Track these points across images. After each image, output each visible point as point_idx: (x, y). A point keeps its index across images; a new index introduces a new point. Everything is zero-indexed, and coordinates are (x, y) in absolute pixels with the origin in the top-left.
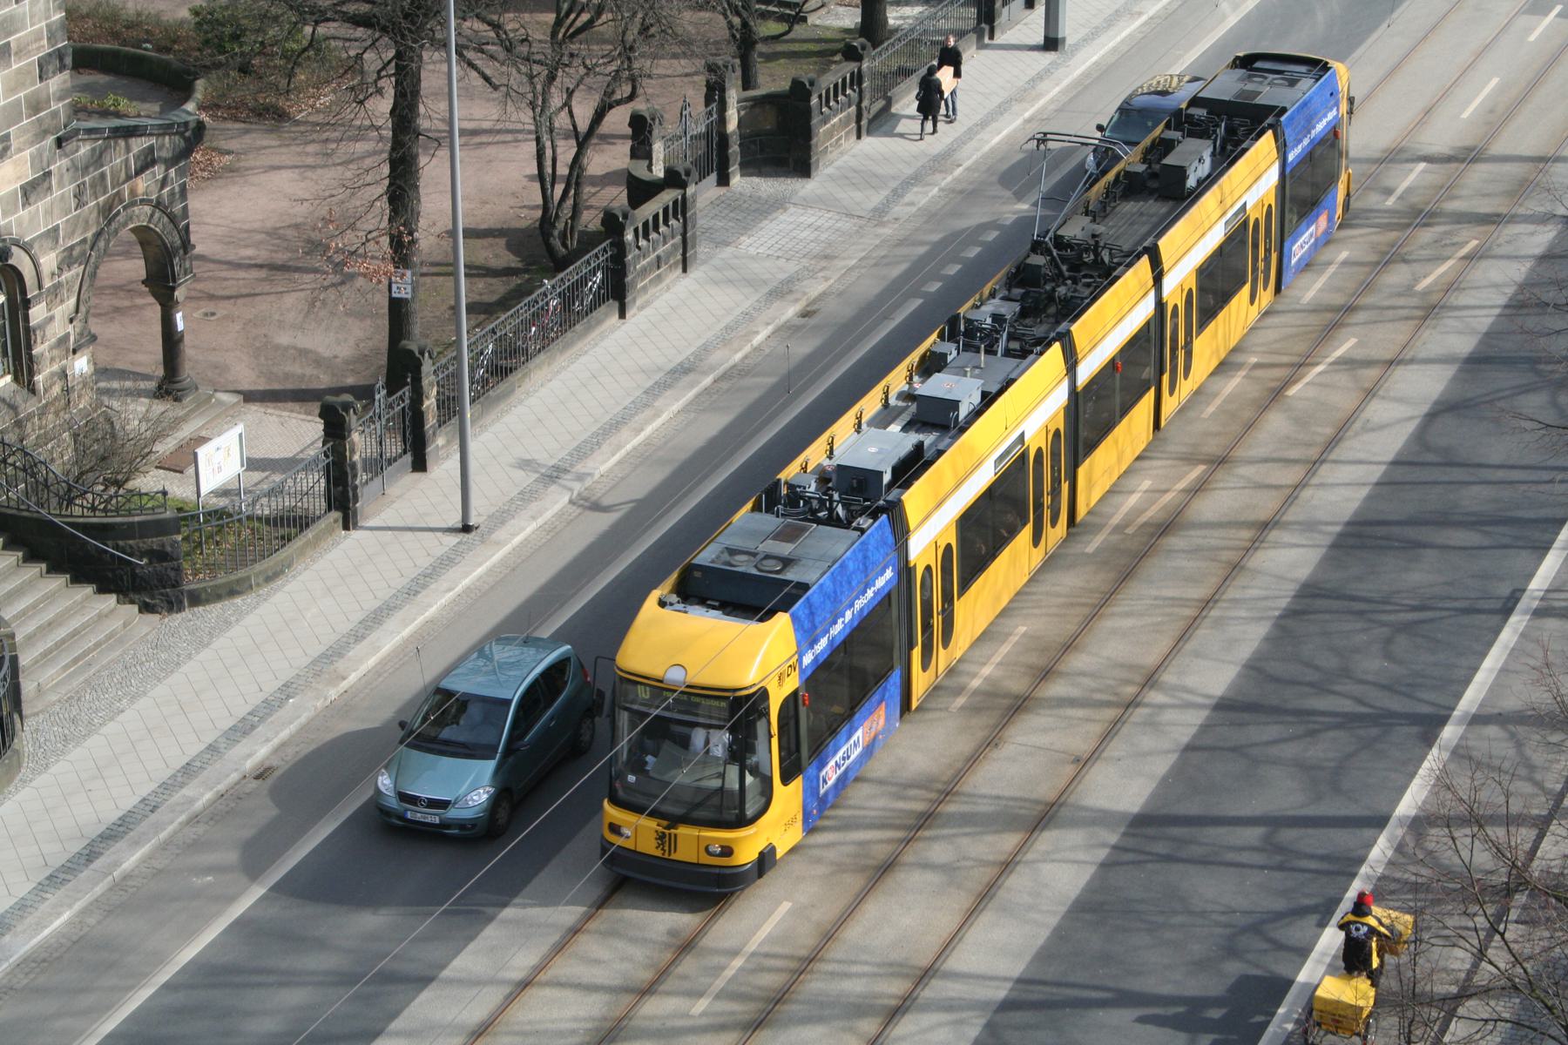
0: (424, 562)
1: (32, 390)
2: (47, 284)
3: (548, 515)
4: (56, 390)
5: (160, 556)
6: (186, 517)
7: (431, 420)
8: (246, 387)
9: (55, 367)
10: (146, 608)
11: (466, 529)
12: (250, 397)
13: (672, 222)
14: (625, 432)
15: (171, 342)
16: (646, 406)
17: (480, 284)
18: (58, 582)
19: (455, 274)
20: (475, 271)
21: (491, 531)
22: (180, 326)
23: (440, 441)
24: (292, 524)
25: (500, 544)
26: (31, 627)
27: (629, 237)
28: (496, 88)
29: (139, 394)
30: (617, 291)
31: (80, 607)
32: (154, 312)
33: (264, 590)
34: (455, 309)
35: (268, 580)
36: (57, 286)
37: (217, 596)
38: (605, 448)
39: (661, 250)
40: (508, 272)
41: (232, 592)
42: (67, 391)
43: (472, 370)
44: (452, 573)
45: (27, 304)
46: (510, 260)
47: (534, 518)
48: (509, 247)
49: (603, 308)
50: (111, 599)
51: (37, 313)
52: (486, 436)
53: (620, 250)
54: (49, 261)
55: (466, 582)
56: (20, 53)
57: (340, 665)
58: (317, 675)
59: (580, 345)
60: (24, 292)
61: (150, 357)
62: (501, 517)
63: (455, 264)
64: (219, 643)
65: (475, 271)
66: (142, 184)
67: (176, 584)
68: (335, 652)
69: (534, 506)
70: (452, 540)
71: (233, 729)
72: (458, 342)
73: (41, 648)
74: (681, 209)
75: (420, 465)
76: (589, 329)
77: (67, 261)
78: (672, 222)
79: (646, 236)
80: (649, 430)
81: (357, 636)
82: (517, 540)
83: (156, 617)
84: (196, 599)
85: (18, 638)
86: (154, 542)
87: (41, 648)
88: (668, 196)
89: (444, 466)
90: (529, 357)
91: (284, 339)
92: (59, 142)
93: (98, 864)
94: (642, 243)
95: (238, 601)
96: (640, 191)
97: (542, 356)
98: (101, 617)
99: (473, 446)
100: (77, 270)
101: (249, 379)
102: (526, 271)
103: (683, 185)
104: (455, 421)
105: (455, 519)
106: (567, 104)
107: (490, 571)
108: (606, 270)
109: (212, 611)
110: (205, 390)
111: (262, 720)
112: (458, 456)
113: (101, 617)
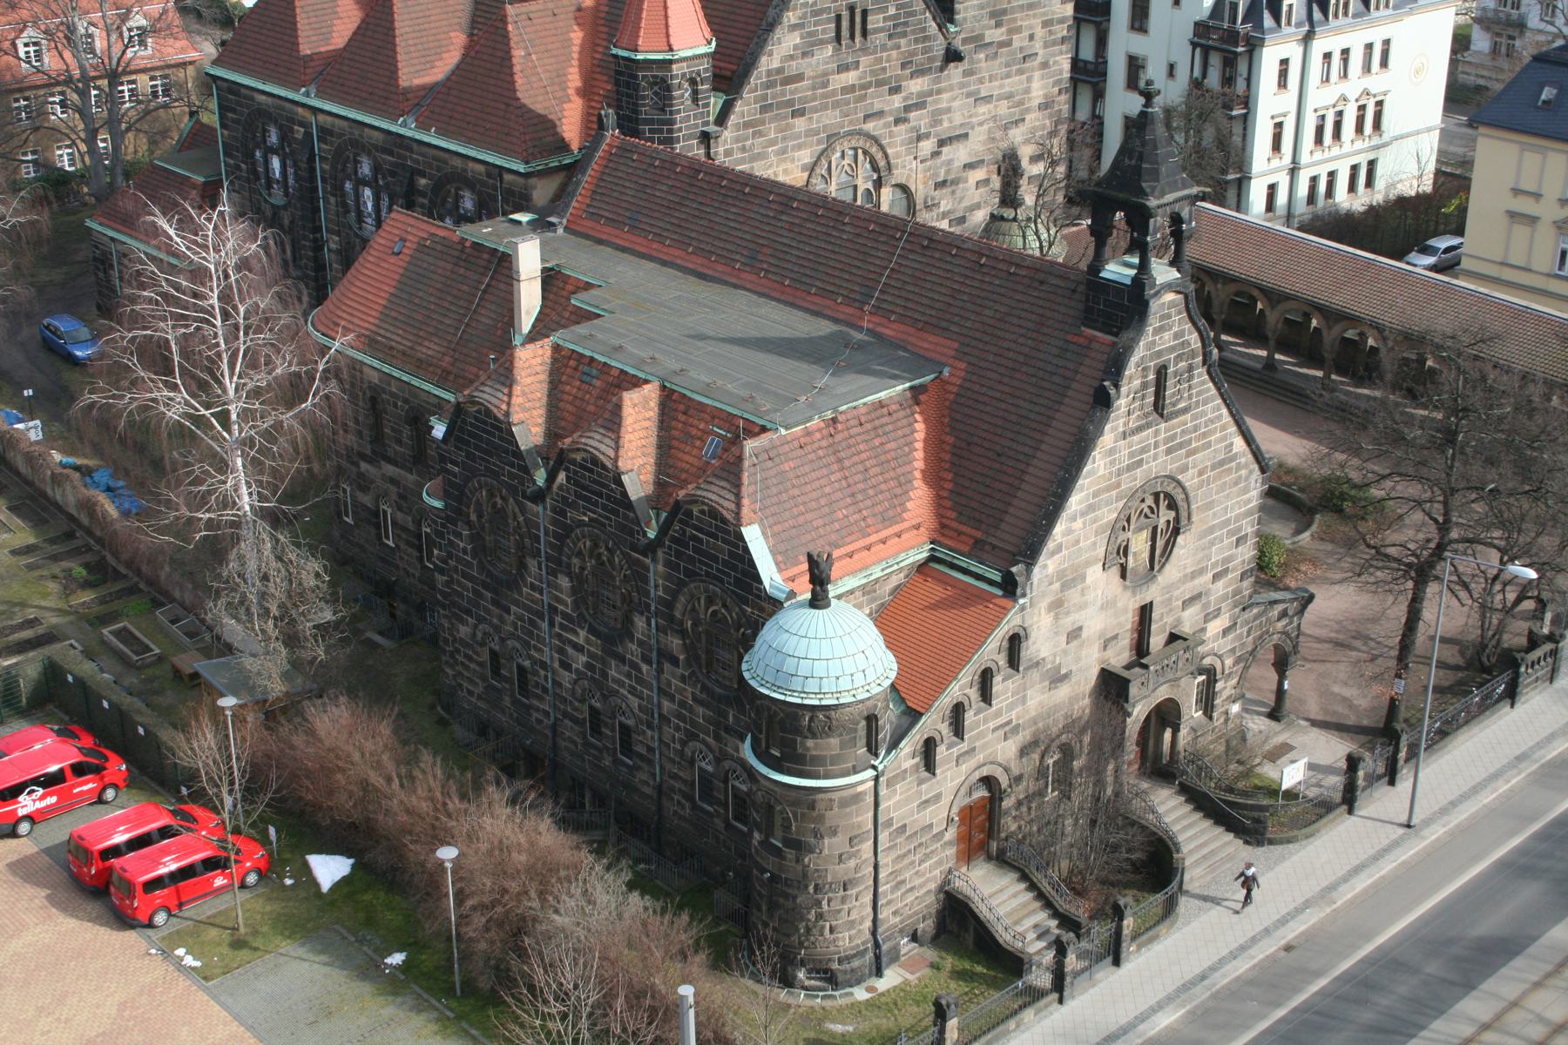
0: (1385, 842)
1: (1211, 718)
2: (1227, 672)
3: (1452, 825)
4: (1222, 720)
5: (1257, 821)
6: (1273, 791)
7: (1401, 762)
8: (1313, 716)
9: (1223, 709)
10: (1247, 842)
11: (1409, 826)
12: (1315, 723)
13: (1549, 659)
14: (1500, 782)
15: (1280, 693)
16: (1515, 767)
17: (1441, 672)
18: (1207, 823)
19: (1430, 665)
20: (1442, 665)
21: (1421, 830)
22: (1286, 687)
23: (1404, 771)
24: (1323, 808)
25: (1424, 838)
26: (1192, 846)
27: (1523, 669)
28: (1463, 605)
29: (1259, 713)
30: (1511, 695)
31: (1216, 838)
32: (1274, 677)
33: (1304, 843)
34: (1426, 688)
35: (1307, 837)
36: (1230, 674)
37: (1281, 842)
38: (1489, 789)
39: (1539, 674)
40: (1457, 668)
41: (1289, 841)
42: (1227, 720)
43: (1428, 734)
44: (1397, 852)
45: (1216, 681)
46: (1460, 661)
47: (1444, 826)
48: (1462, 653)
49: (1502, 703)
50: (1231, 836)
51: (1219, 686)
52: (1428, 770)
53: (1517, 675)
54: (1229, 662)
55: (1404, 858)
56: (1234, 570)
57: (1334, 894)
58: (1322, 897)
59: (1486, 722)
60: (1215, 675)
61: (1270, 699)
62: (1428, 822)
63: (1431, 658)
64: (1279, 869)
65: (1442, 665)
66: (1280, 625)
67: (1263, 834)
68: (1332, 887)
69: (1446, 818)
70: (1401, 831)
71: (1278, 920)
72: (1424, 709)
73: (1196, 856)
74: (1554, 653)
75: (1392, 782)
76: (1493, 714)
77: (1236, 663)
78: (1549, 659)
79: (1532, 667)
80: (1514, 781)
81: (1345, 879)
82: (1433, 837)
83: (1250, 848)
84: (1271, 842)
85: (1187, 863)
86: (1256, 814)
87: (1196, 856)
88: (1548, 647)
89: (1404, 785)
90: (1459, 727)
91: (1336, 689)
92: (1244, 609)
93: (1206, 983)
94: (1530, 671)
95: (1291, 846)
96: (1533, 642)
97: (1465, 728)
98: (1226, 844)
99: (1420, 775)
100: (1242, 665)
101: (1314, 710)
102: (1466, 669)
103: (1558, 642)
104: (1414, 761)
105: (1403, 819)
106: (1503, 591)
107: (1417, 853)
108: (1507, 684)
109: (1277, 850)
110: (1292, 716)
111: (1293, 918)
112: (1412, 780)
113: (1226, 844)
